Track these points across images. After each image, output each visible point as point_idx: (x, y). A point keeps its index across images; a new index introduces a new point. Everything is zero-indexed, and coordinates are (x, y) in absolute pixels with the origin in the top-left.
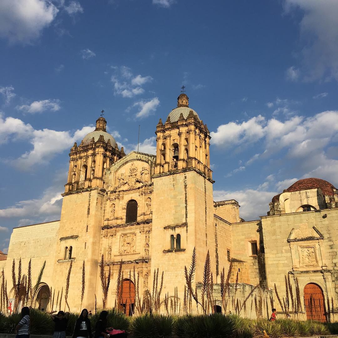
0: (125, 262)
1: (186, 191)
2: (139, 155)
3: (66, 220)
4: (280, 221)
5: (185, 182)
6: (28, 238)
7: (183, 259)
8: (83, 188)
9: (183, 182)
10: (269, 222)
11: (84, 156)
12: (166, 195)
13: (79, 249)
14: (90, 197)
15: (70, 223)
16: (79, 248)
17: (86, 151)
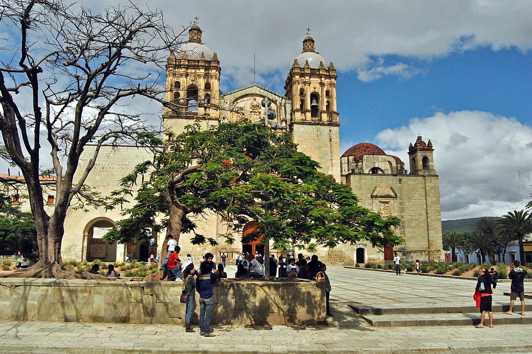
2: (262, 91)
4: (366, 179)
6: (108, 160)
8: (197, 114)
10: (357, 179)
11: (192, 73)
12: (309, 144)
17: (197, 67)
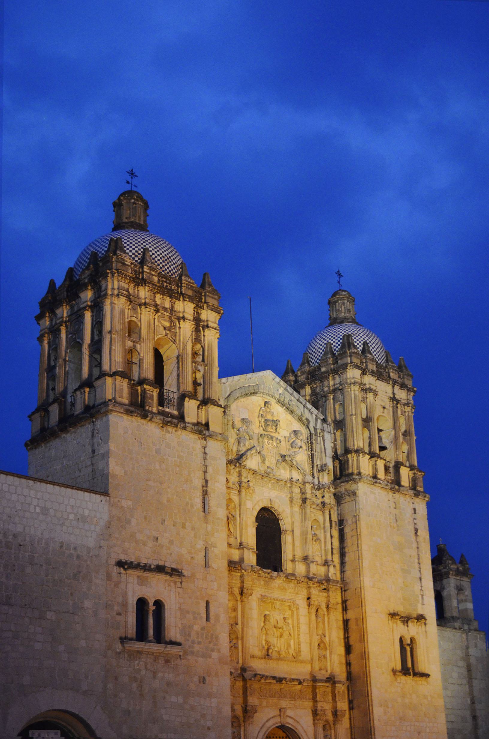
0: (285, 679)
1: (418, 544)
3: (130, 503)
5: (415, 521)
7: (425, 697)
9: (411, 520)
11: (165, 309)
13: (190, 616)
14: (205, 459)
15: (145, 518)
16: (188, 612)
